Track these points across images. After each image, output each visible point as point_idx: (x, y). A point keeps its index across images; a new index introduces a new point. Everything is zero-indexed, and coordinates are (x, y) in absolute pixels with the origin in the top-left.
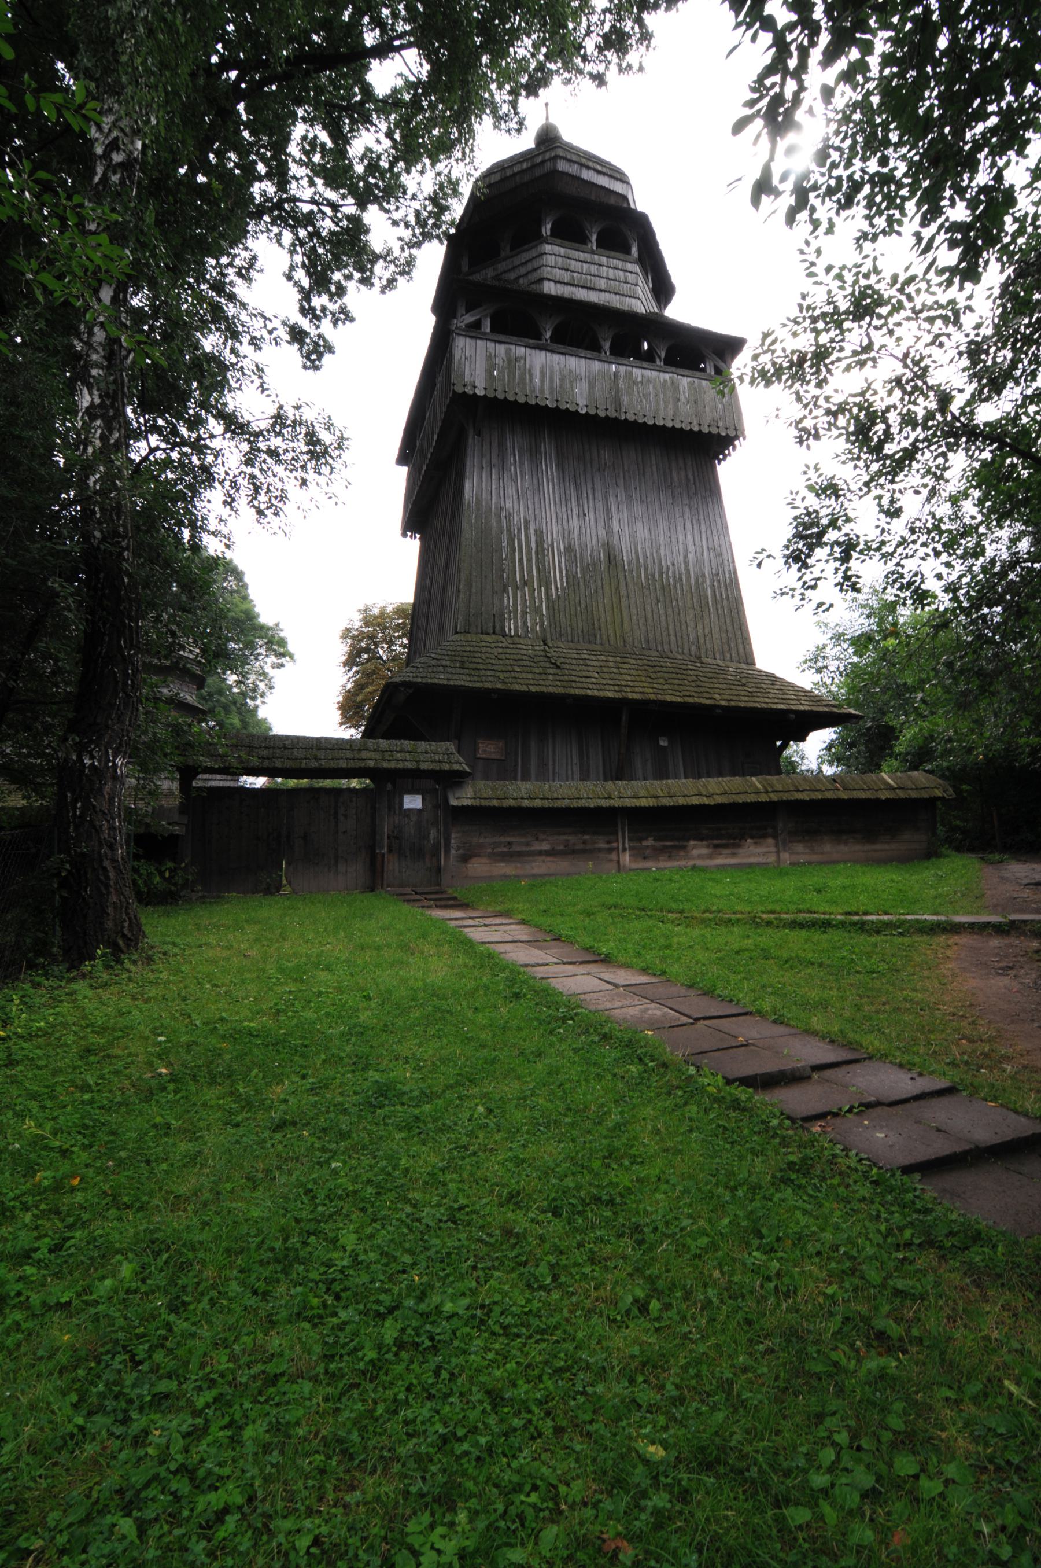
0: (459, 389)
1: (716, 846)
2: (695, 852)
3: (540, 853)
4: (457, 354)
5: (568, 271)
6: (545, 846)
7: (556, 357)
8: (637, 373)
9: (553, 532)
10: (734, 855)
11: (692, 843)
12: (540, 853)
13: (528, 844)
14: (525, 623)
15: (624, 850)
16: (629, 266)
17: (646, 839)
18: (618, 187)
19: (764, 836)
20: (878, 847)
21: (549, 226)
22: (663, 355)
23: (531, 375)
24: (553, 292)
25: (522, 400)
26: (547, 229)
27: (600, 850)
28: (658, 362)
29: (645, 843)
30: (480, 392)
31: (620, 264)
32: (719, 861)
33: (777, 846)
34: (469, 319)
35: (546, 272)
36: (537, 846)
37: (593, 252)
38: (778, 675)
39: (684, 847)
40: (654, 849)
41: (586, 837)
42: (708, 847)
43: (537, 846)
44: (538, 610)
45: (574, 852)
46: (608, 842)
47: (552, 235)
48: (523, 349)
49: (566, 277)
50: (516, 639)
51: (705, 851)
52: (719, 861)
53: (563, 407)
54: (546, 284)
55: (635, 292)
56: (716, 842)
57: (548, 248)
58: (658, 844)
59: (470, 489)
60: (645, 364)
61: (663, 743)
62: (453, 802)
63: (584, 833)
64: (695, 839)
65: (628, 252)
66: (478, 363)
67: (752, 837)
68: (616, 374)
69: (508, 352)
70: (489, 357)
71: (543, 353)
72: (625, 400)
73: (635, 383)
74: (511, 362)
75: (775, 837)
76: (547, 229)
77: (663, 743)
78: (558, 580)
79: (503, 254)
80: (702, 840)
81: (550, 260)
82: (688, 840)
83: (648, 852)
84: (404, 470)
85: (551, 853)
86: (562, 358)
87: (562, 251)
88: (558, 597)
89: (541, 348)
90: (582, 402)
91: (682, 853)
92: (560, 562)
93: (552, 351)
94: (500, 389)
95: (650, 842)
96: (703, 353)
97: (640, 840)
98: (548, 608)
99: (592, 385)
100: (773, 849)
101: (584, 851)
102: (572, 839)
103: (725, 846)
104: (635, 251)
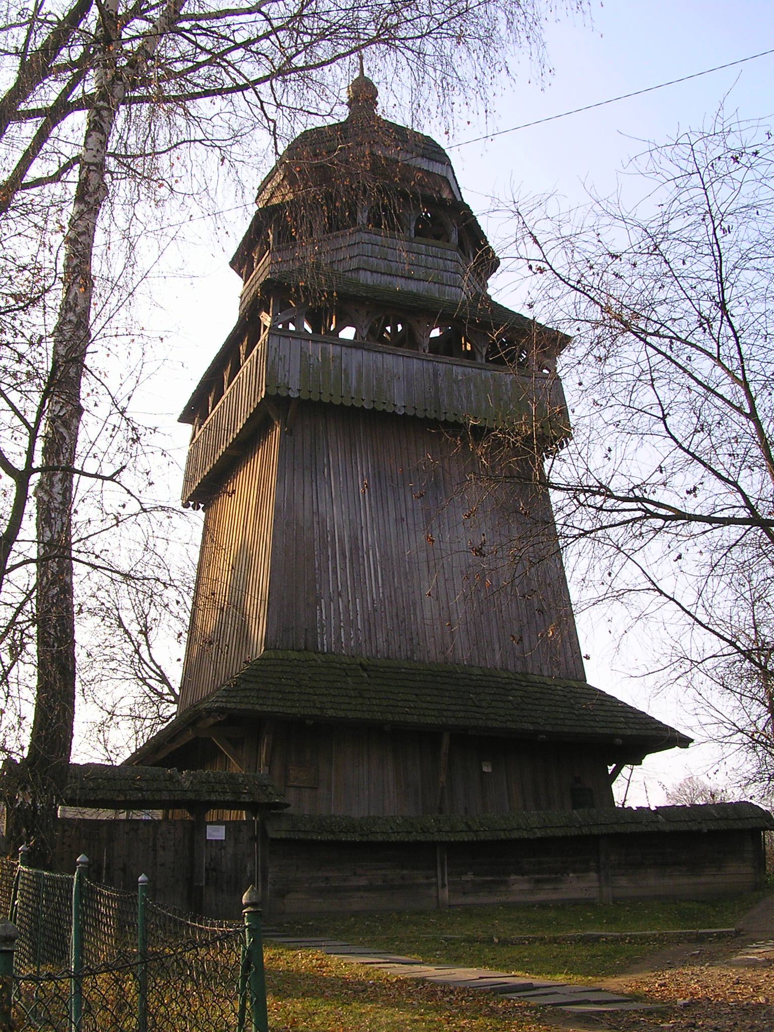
1: (538, 881)
2: (516, 887)
3: (358, 889)
6: (363, 882)
8: (458, 371)
11: (513, 877)
12: (358, 889)
14: (339, 638)
15: (443, 886)
16: (449, 254)
17: (466, 873)
18: (437, 169)
19: (587, 870)
20: (703, 879)
23: (347, 376)
24: (370, 282)
25: (337, 401)
28: (479, 361)
30: (294, 394)
31: (439, 252)
33: (599, 880)
41: (405, 872)
44: (351, 624)
46: (427, 878)
48: (338, 348)
49: (382, 265)
51: (526, 886)
52: (541, 897)
53: (380, 408)
55: (455, 280)
56: (537, 876)
58: (479, 879)
61: (487, 769)
62: (272, 835)
64: (517, 873)
67: (574, 872)
71: (359, 352)
72: (445, 399)
73: (457, 382)
75: (598, 871)
80: (523, 875)
85: (368, 889)
86: (379, 356)
88: (375, 610)
90: (400, 403)
93: (368, 350)
95: (469, 877)
96: (529, 346)
98: (363, 619)
100: (597, 884)
103: (547, 881)
104: (454, 237)
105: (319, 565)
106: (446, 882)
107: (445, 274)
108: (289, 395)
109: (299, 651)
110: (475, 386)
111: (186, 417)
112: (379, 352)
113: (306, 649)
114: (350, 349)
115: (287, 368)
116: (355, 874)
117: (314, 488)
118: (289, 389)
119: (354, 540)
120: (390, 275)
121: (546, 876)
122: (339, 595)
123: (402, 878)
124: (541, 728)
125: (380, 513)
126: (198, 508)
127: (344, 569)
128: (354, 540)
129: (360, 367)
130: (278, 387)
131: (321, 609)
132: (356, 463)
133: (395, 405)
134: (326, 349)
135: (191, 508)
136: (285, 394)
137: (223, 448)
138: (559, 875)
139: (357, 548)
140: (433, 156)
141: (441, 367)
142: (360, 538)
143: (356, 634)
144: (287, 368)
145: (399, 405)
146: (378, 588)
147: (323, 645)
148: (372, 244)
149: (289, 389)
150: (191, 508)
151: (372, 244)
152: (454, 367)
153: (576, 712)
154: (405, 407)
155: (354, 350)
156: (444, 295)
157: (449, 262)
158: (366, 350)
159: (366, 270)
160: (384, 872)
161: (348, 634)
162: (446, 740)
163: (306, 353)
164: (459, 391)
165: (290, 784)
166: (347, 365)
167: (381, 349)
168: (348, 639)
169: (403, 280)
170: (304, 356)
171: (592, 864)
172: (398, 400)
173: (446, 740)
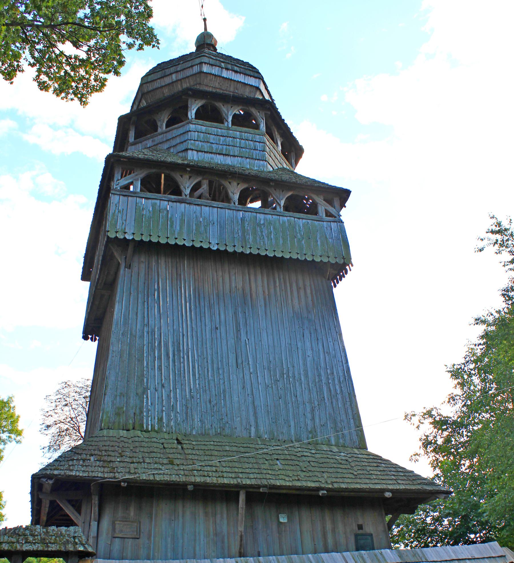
0: (112, 235)
18: (252, 81)
21: (194, 112)
22: (282, 203)
23: (172, 223)
24: (195, 158)
26: (192, 113)
31: (250, 136)
34: (124, 182)
37: (228, 129)
38: (385, 457)
47: (196, 118)
49: (206, 147)
50: (153, 434)
54: (190, 152)
57: (192, 127)
65: (257, 127)
68: (243, 219)
69: (153, 205)
73: (259, 225)
76: (192, 113)
79: (159, 130)
86: (198, 208)
87: (204, 128)
88: (192, 397)
89: (181, 202)
92: (194, 367)
93: (190, 204)
98: (182, 405)
104: (263, 126)
105: (147, 364)
107: (254, 151)
109: (128, 430)
110: (274, 228)
112: (198, 205)
113: (134, 429)
114: (175, 203)
115: (124, 218)
117: (146, 306)
119: (177, 345)
120: (211, 153)
122: (163, 386)
124: (323, 486)
125: (199, 324)
126: (95, 340)
127: (168, 367)
128: (177, 345)
129: (183, 215)
130: (117, 232)
131: (147, 397)
132: (181, 288)
133: (210, 243)
134: (156, 204)
136: (122, 237)
139: (179, 351)
140: (248, 72)
143: (176, 416)
144: (124, 218)
145: (213, 242)
146: (195, 380)
147: (147, 425)
148: (198, 132)
149: (125, 233)
151: (198, 132)
152: (258, 215)
153: (355, 473)
154: (218, 244)
155: (178, 204)
156: (254, 167)
157: (258, 143)
158: (187, 203)
159: (192, 150)
161: (168, 415)
162: (242, 497)
164: (262, 232)
165: (116, 535)
167: (199, 203)
168: (169, 420)
169: (222, 157)
170: (138, 209)
173: (242, 497)
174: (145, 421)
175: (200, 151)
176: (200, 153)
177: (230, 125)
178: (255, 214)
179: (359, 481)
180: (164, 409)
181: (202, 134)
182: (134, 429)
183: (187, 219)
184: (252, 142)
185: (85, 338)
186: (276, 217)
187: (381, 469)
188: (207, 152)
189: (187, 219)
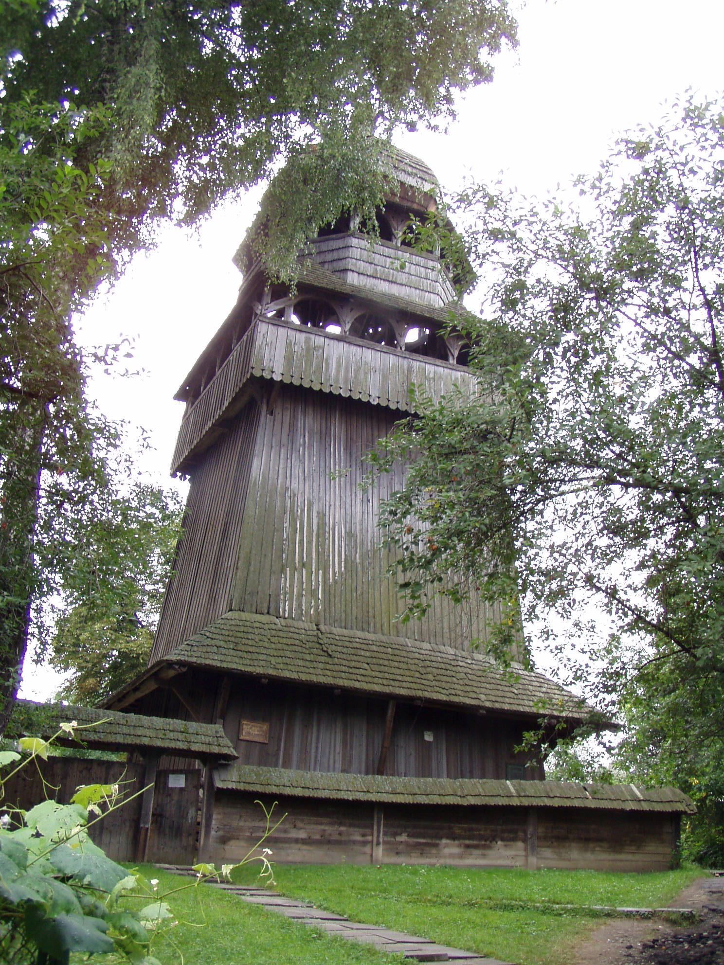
0: (257, 374)
1: (468, 846)
2: (447, 851)
3: (297, 841)
4: (259, 340)
5: (374, 268)
6: (302, 835)
7: (354, 349)
9: (335, 516)
10: (484, 856)
11: (444, 841)
12: (297, 841)
13: (285, 831)
14: (300, 605)
15: (378, 844)
16: (431, 264)
17: (400, 834)
19: (514, 839)
20: (622, 856)
23: (327, 364)
24: (356, 283)
25: (316, 388)
27: (354, 842)
29: (399, 839)
30: (277, 378)
31: (422, 261)
32: (469, 861)
33: (526, 850)
35: (350, 264)
36: (294, 834)
37: (397, 249)
39: (436, 846)
40: (407, 844)
41: (343, 829)
42: (460, 846)
43: (294, 834)
44: (313, 593)
45: (329, 842)
46: (363, 835)
48: (322, 339)
49: (370, 270)
50: (290, 621)
51: (456, 850)
53: (356, 397)
54: (350, 274)
55: (434, 288)
56: (467, 842)
57: (354, 241)
59: (258, 467)
60: (439, 362)
62: (219, 784)
63: (340, 824)
64: (447, 838)
66: (280, 348)
67: (502, 840)
69: (307, 341)
70: (289, 345)
71: (341, 344)
74: (310, 350)
75: (524, 841)
77: (428, 737)
78: (337, 565)
80: (454, 839)
81: (355, 253)
82: (441, 838)
83: (401, 847)
84: (182, 406)
86: (359, 349)
88: (335, 581)
90: (374, 393)
91: (434, 851)
93: (350, 343)
94: (296, 376)
95: (403, 838)
97: (395, 835)
98: (324, 591)
99: (385, 378)
100: (523, 853)
101: (338, 843)
102: (329, 829)
103: (476, 847)
106: (381, 840)
107: (425, 281)
108: (272, 378)
110: (444, 384)
111: (182, 395)
112: (359, 346)
114: (332, 341)
116: (295, 827)
117: (289, 465)
118: (273, 372)
121: (475, 842)
123: (340, 834)
124: (481, 704)
125: (348, 493)
130: (263, 370)
134: (310, 339)
135: (178, 478)
136: (269, 377)
137: (210, 424)
138: (488, 842)
141: (416, 364)
142: (327, 514)
145: (373, 396)
147: (284, 610)
149: (273, 372)
150: (178, 478)
153: (516, 691)
159: (353, 271)
160: (323, 827)
163: (291, 342)
166: (328, 356)
167: (361, 343)
171: (521, 834)
172: (373, 392)
174: (282, 606)
175: (362, 274)
176: (361, 277)
177: (399, 245)
178: (423, 364)
179: (522, 702)
180: (304, 593)
181: (366, 252)
182: (268, 613)
183: (343, 361)
184: (423, 269)
185: (174, 475)
186: (449, 370)
187: (544, 690)
188: (370, 276)
189: (343, 361)
